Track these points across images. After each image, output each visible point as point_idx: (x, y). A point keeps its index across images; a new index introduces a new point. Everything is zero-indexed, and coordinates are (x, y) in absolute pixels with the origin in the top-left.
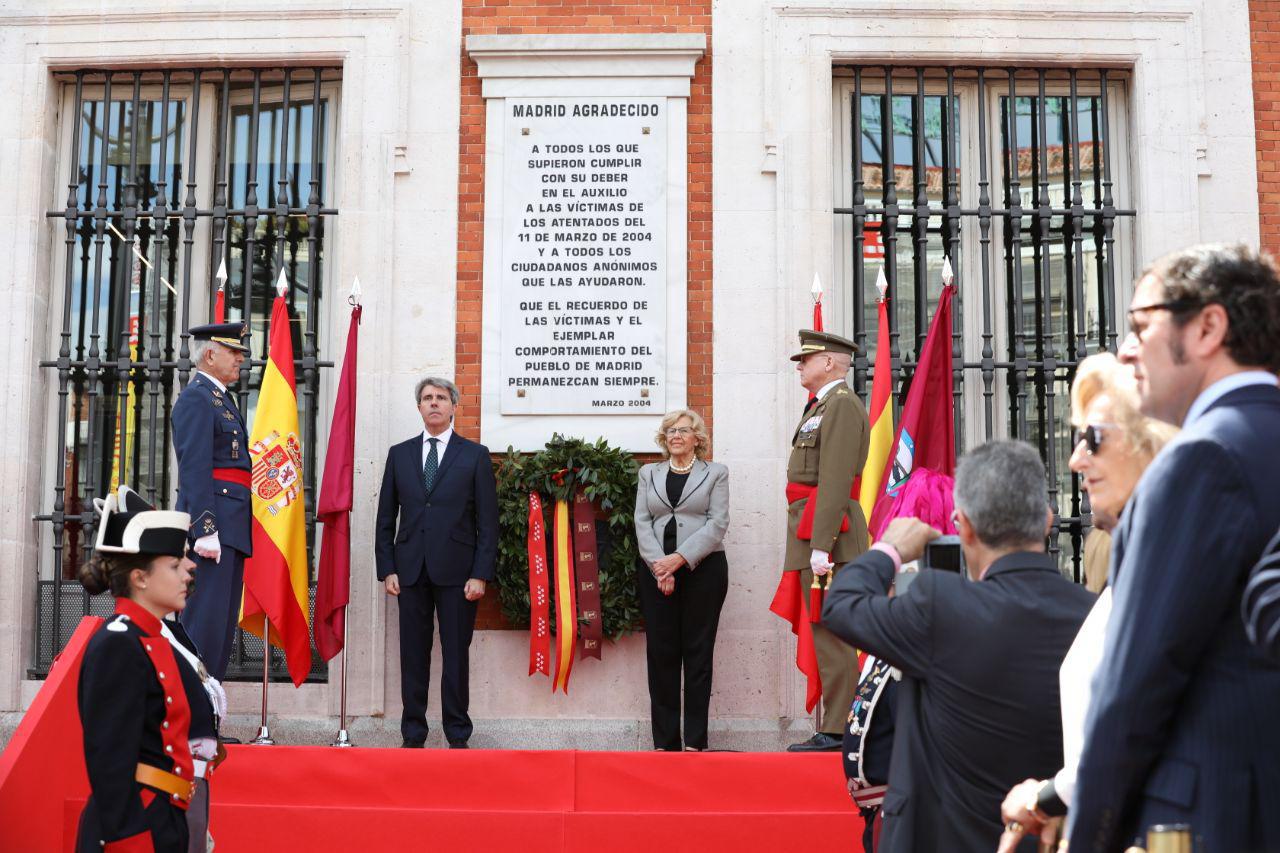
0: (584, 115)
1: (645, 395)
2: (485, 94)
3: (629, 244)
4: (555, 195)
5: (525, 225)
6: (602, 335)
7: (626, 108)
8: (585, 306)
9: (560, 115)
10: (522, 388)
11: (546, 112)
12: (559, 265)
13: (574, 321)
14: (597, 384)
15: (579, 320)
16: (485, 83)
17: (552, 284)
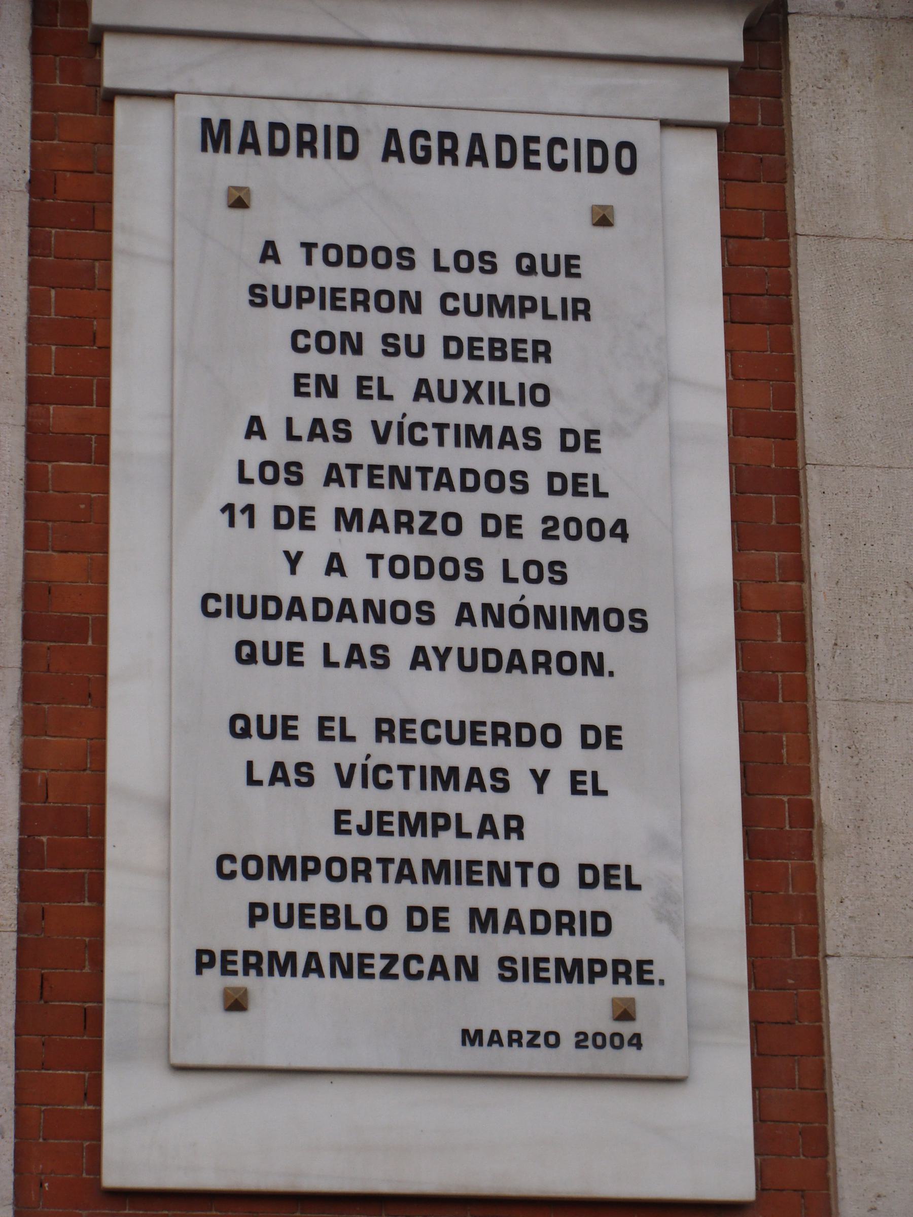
0: (417, 160)
1: (625, 1013)
2: (109, 81)
3: (561, 549)
4: (333, 393)
5: (243, 479)
6: (487, 826)
7: (543, 147)
8: (432, 732)
9: (344, 155)
10: (239, 981)
11: (302, 145)
12: (347, 602)
13: (397, 777)
14: (473, 976)
15: (415, 777)
16: (112, 47)
17: (329, 663)
